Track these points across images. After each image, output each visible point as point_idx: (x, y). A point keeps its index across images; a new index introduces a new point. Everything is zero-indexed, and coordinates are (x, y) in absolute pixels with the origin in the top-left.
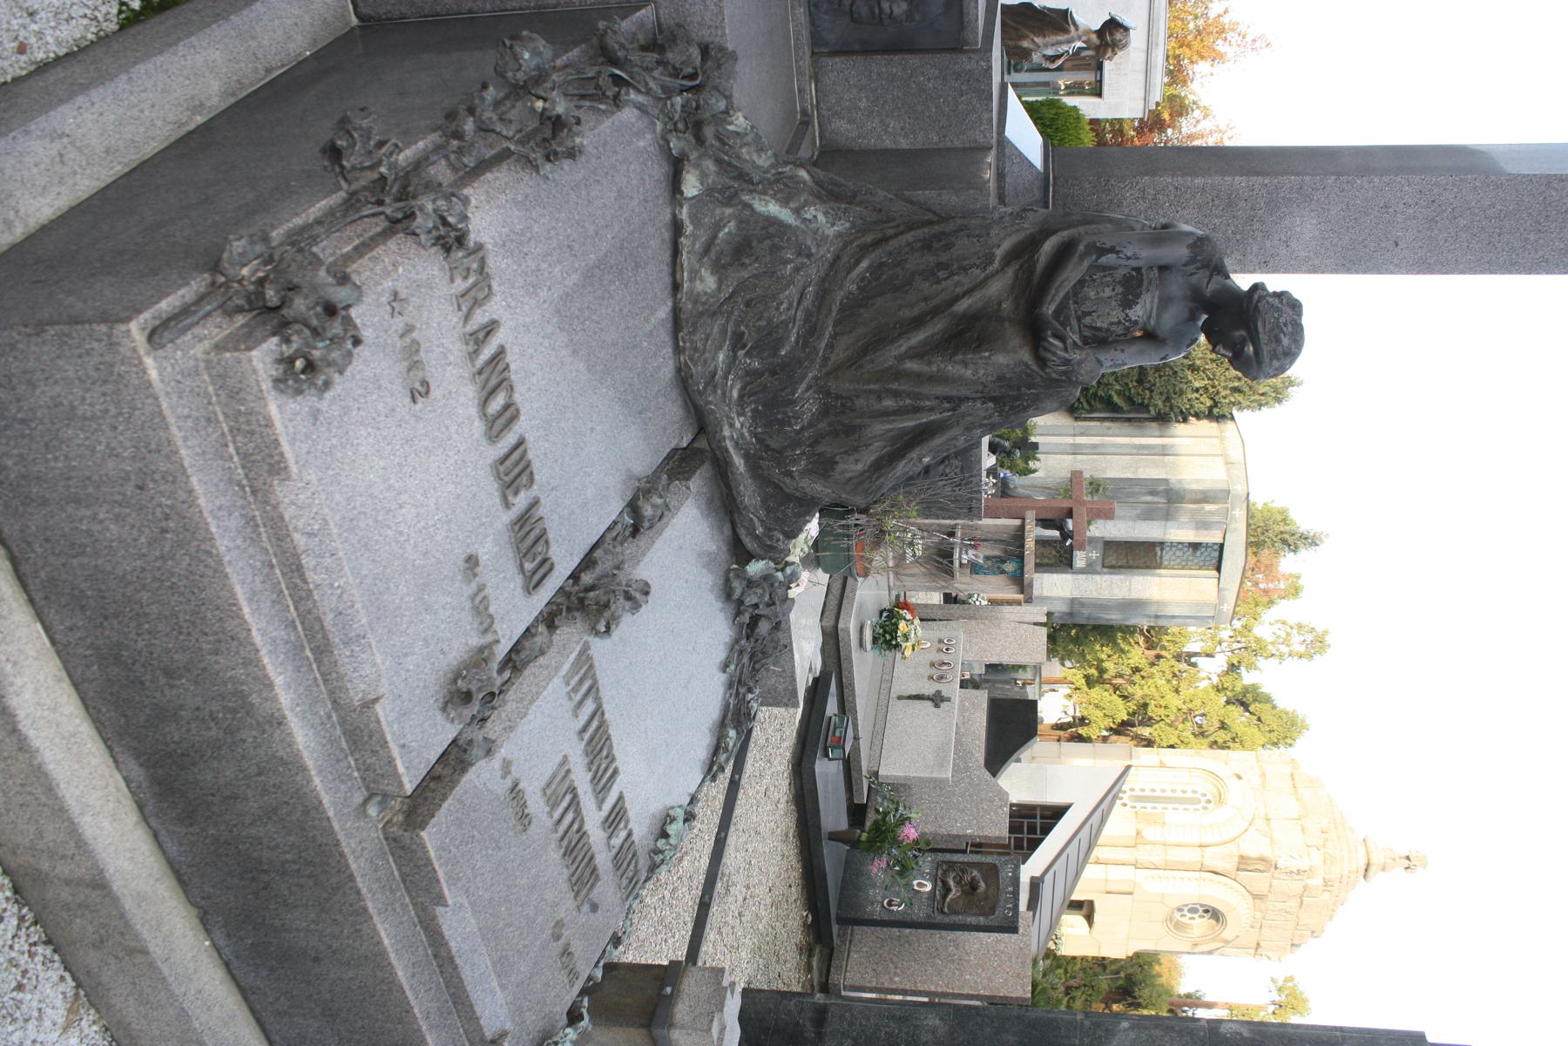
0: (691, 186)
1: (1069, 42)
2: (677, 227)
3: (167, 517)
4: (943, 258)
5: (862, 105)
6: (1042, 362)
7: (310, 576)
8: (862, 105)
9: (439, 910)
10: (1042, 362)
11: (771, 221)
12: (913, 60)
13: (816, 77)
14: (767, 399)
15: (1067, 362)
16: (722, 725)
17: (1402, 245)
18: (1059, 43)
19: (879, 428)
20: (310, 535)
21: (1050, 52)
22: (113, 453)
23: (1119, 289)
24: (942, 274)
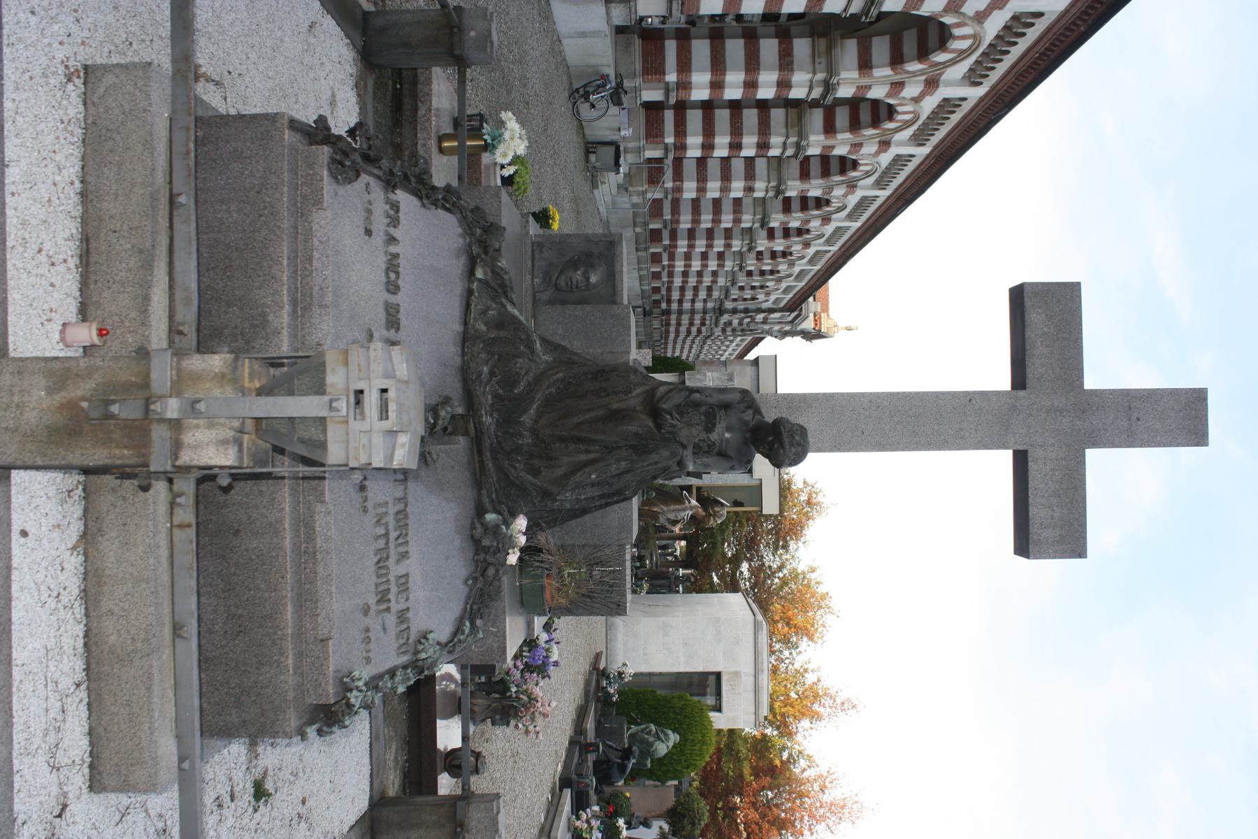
0: (479, 274)
1: (684, 510)
2: (470, 292)
3: (265, 208)
4: (604, 385)
5: (560, 332)
6: (659, 426)
7: (315, 262)
8: (560, 332)
9: (319, 508)
10: (659, 426)
11: (514, 317)
12: (588, 308)
13: (534, 316)
14: (509, 409)
15: (673, 426)
16: (461, 620)
17: (866, 433)
18: (679, 510)
19: (566, 459)
20: (321, 242)
21: (672, 516)
22: (252, 175)
23: (703, 418)
24: (603, 394)
